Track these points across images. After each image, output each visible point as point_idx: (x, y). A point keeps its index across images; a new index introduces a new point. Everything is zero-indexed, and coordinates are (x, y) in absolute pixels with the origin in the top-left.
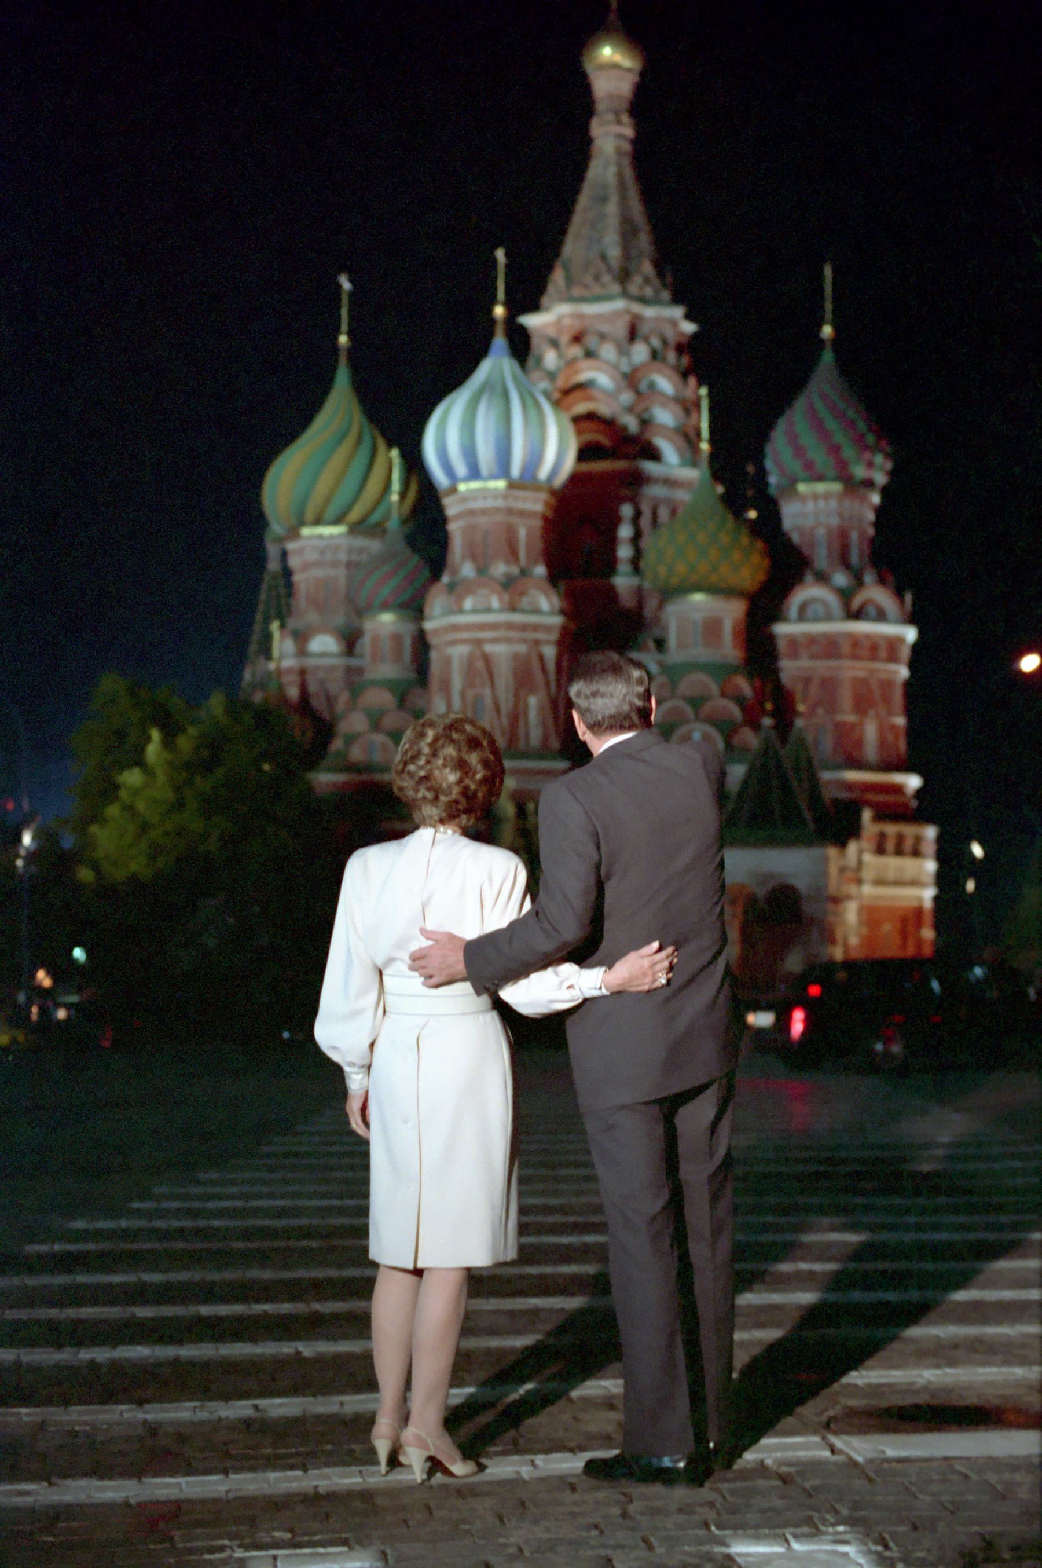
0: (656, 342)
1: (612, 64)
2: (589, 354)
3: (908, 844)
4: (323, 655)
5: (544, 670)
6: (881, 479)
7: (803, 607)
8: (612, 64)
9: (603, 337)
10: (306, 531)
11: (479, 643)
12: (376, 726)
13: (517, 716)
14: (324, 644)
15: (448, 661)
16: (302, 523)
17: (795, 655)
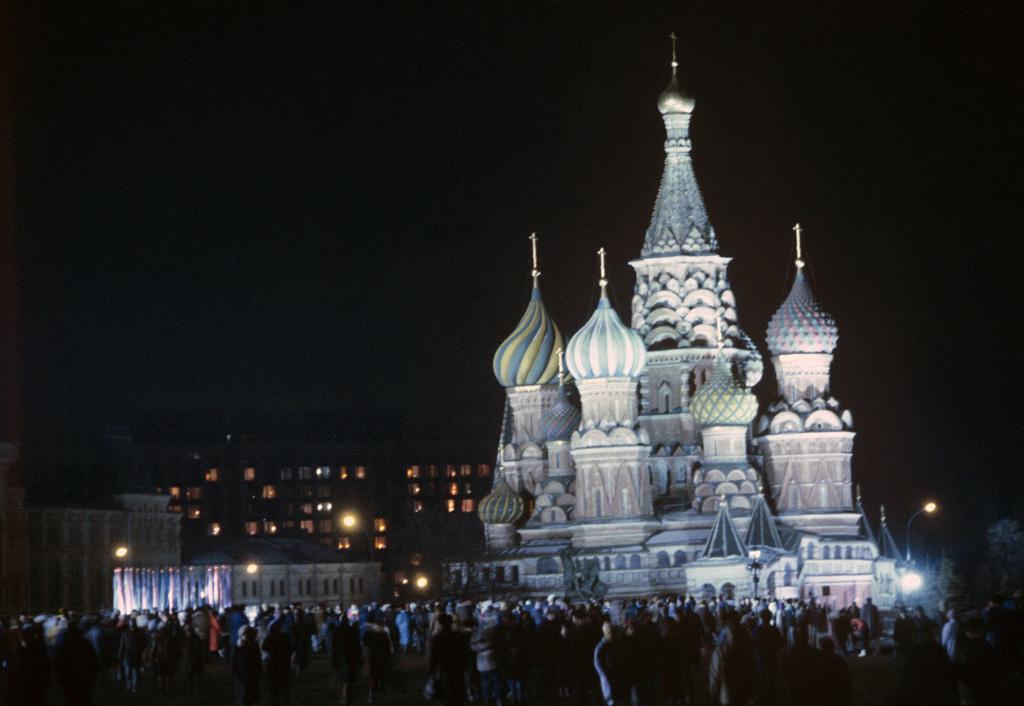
0: (701, 276)
1: (677, 112)
2: (664, 287)
3: (843, 553)
4: (531, 458)
5: (631, 476)
6: (830, 348)
7: (783, 425)
8: (677, 112)
9: (671, 276)
10: (517, 389)
11: (597, 462)
12: (554, 502)
13: (618, 498)
14: (532, 451)
15: (583, 471)
16: (516, 385)
17: (779, 453)
